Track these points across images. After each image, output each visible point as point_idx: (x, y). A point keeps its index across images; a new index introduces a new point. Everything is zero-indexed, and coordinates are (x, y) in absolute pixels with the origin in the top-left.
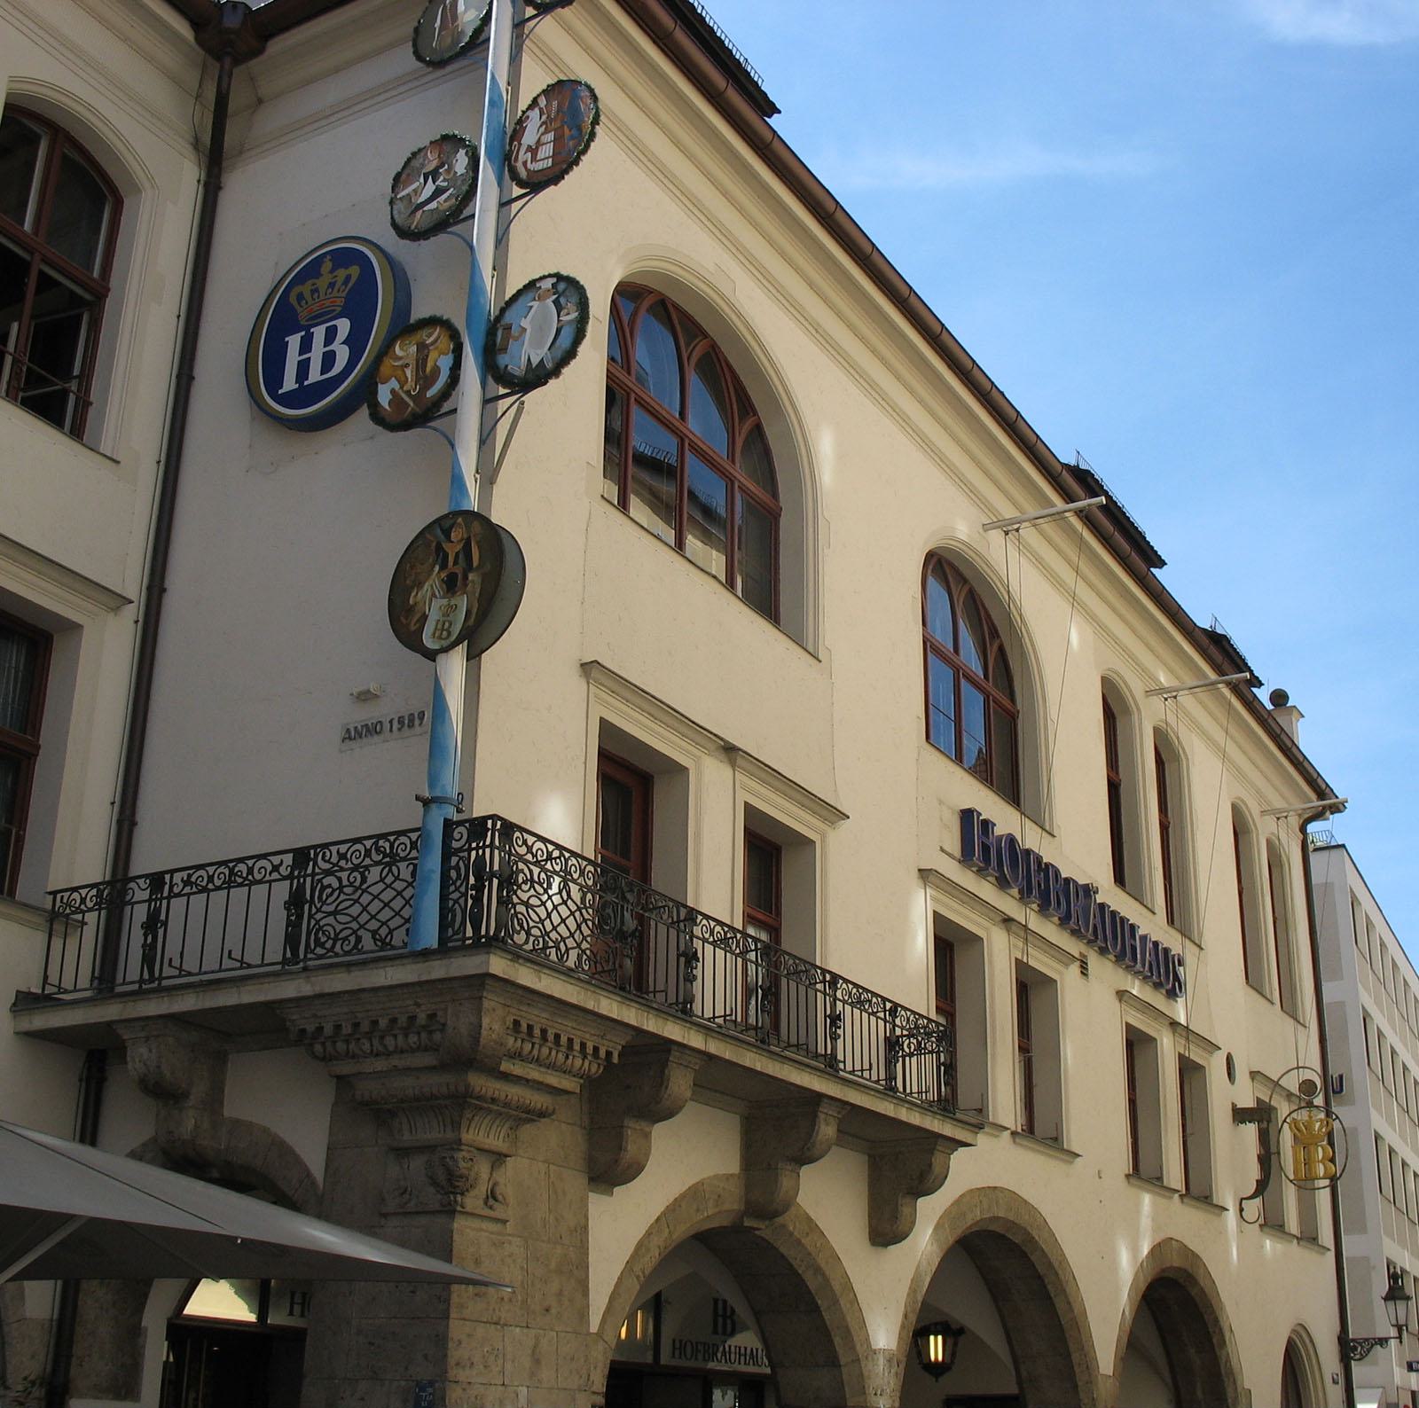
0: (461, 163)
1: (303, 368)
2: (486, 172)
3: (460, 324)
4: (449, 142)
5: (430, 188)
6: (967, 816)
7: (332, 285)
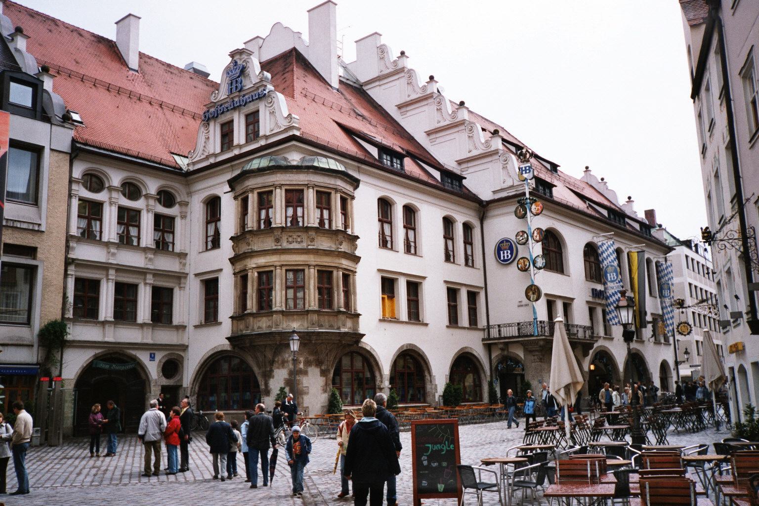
0: (526, 236)
1: (504, 257)
2: (530, 238)
3: (529, 259)
4: (524, 232)
5: (521, 238)
6: (593, 289)
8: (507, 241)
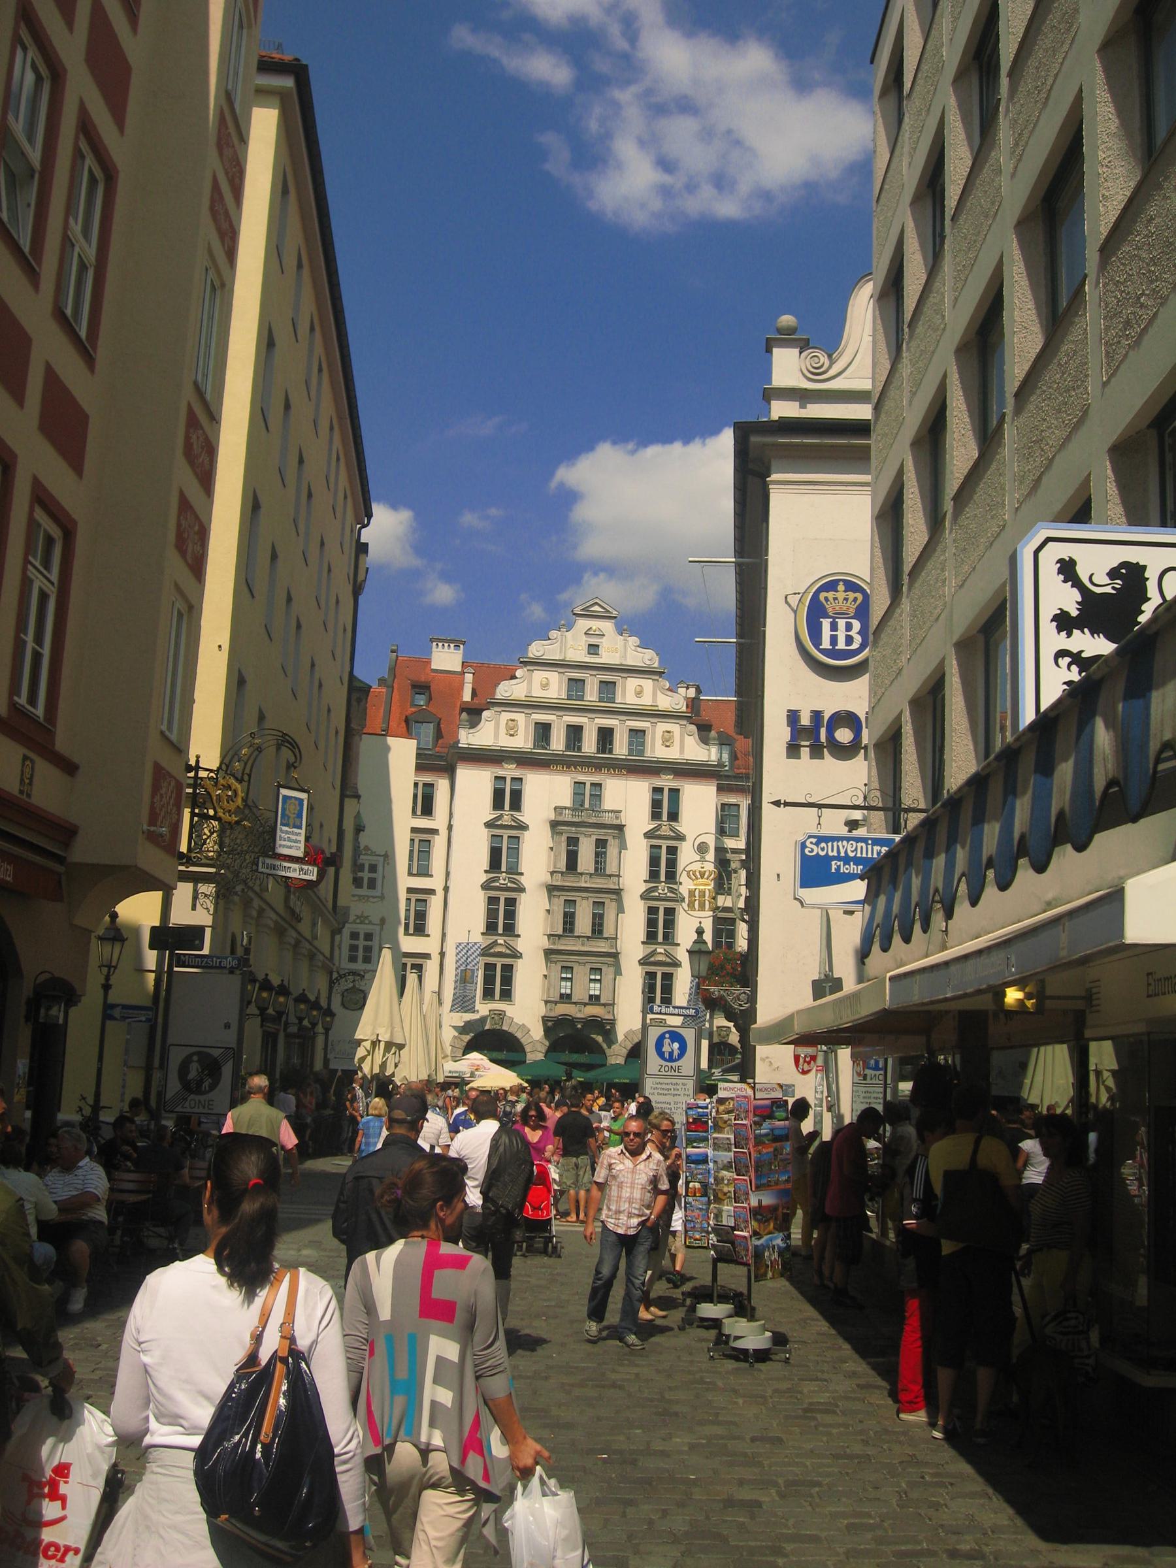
1: (834, 640)
7: (846, 599)
8: (851, 587)
